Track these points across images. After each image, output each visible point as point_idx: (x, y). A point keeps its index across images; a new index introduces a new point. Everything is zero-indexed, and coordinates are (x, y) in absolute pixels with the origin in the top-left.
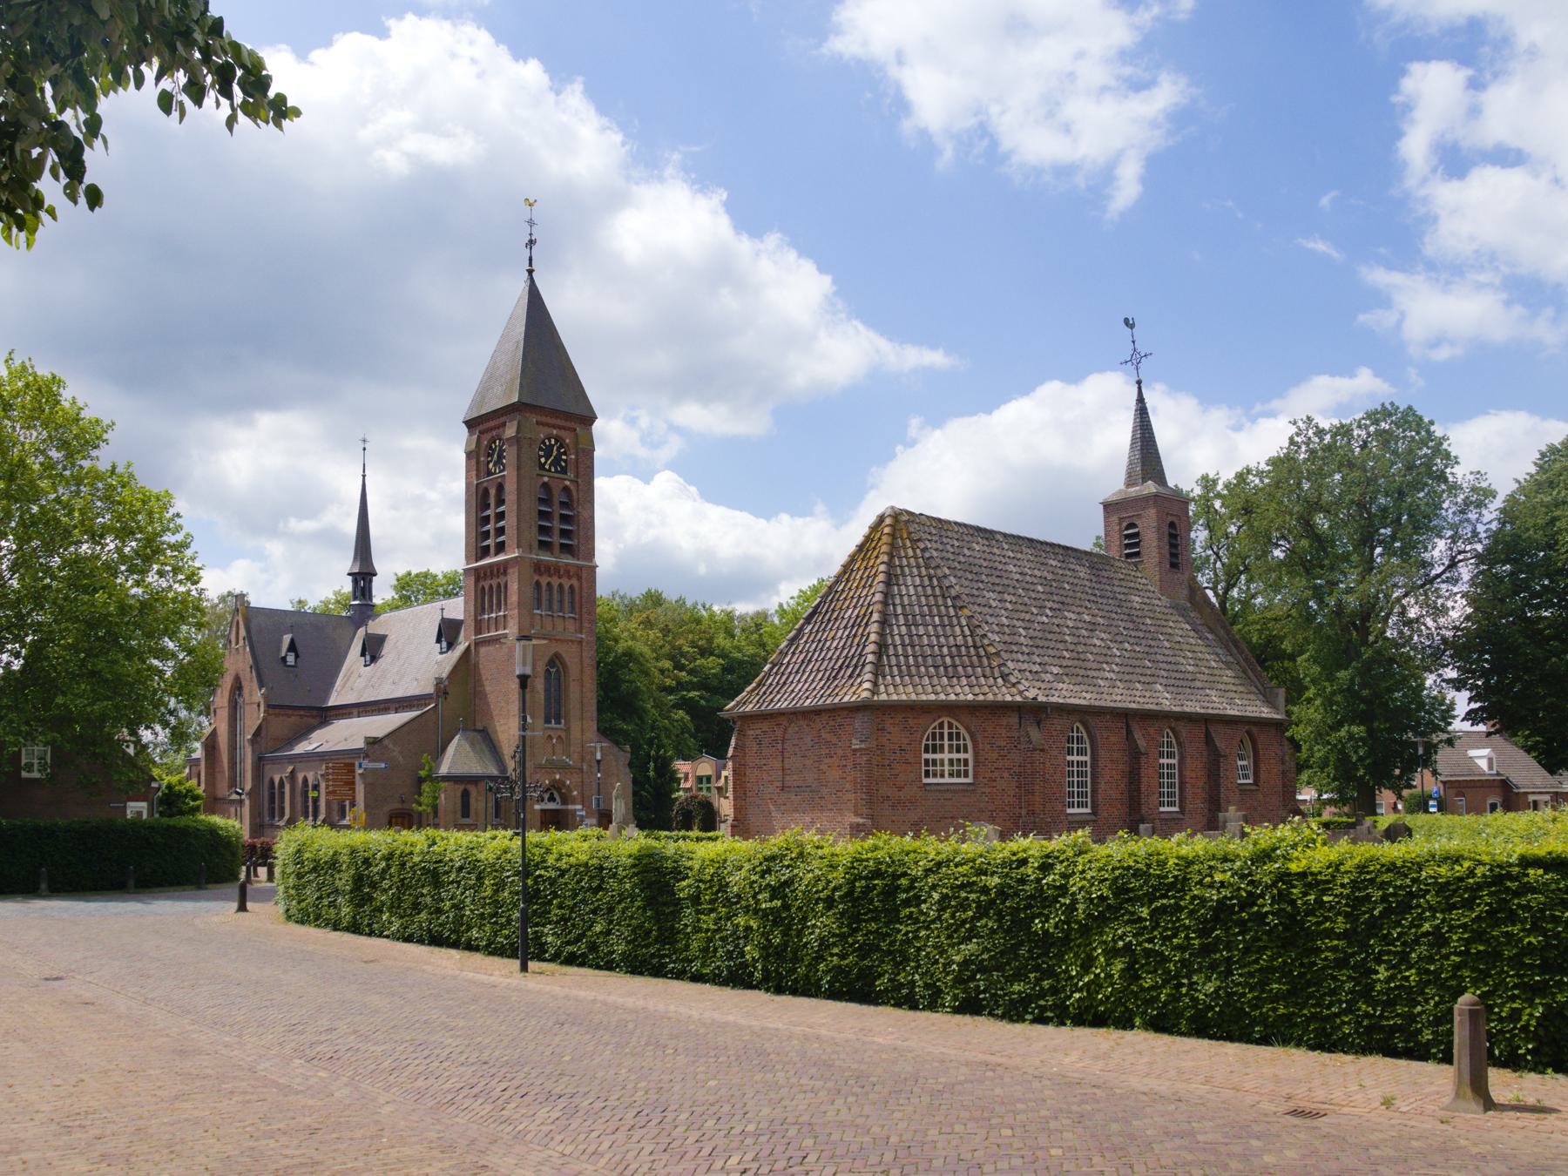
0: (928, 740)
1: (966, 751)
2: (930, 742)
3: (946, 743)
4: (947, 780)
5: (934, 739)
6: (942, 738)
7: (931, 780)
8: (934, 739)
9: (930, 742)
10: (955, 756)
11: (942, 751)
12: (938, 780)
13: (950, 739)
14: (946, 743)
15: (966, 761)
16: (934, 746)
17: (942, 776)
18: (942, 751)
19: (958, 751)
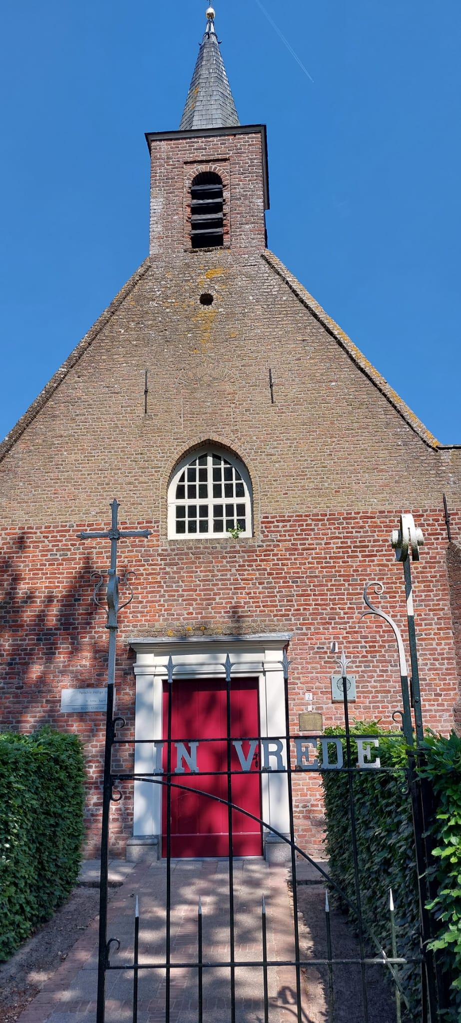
0: (182, 479)
1: (240, 494)
2: (186, 483)
3: (210, 483)
4: (211, 534)
5: (192, 478)
6: (203, 475)
7: (187, 536)
8: (192, 478)
9: (186, 483)
10: (224, 501)
11: (204, 494)
12: (198, 535)
13: (217, 475)
14: (210, 483)
15: (241, 509)
16: (192, 489)
17: (204, 528)
18: (204, 494)
19: (229, 494)
